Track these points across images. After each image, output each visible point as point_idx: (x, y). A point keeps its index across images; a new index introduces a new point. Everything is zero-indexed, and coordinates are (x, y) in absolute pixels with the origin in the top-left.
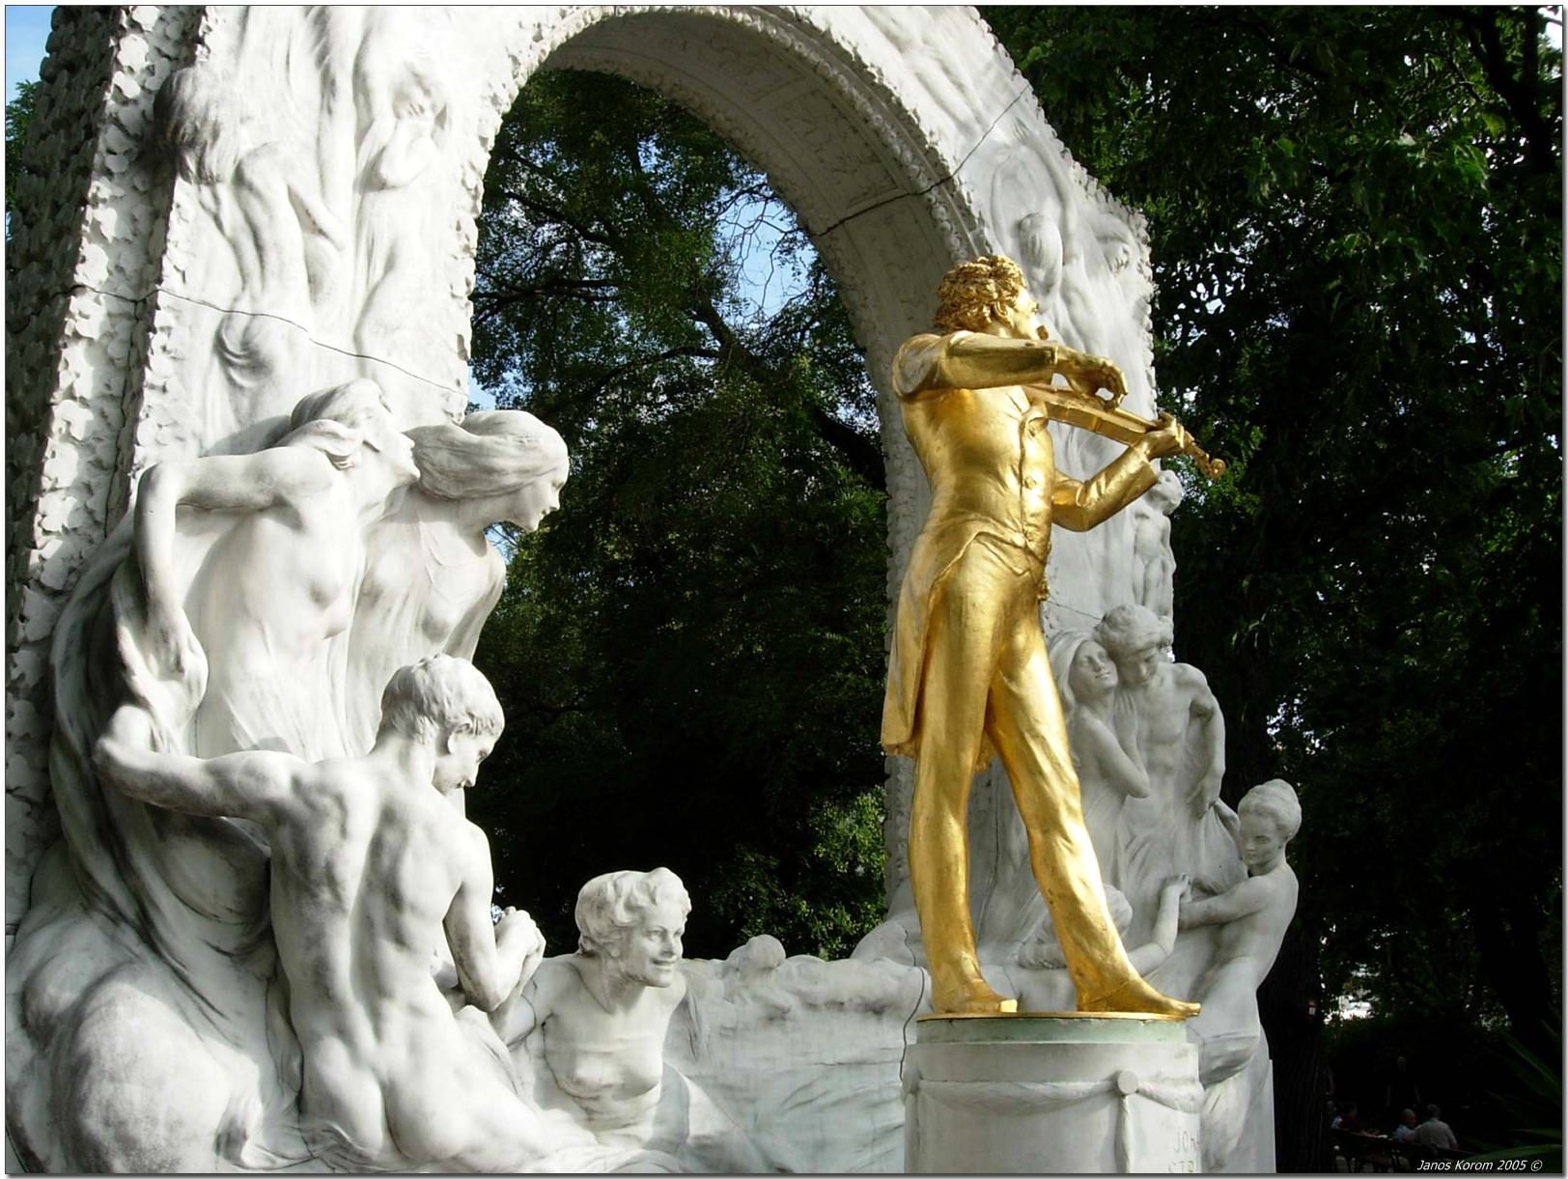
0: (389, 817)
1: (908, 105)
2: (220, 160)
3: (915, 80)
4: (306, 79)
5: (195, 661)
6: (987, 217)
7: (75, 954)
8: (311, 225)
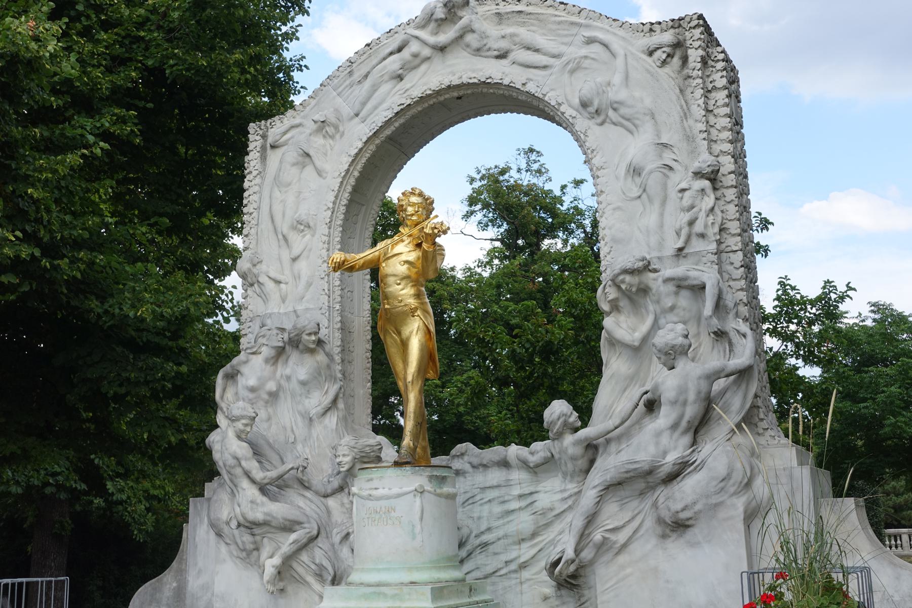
1: (506, 82)
3: (514, 65)
8: (278, 282)
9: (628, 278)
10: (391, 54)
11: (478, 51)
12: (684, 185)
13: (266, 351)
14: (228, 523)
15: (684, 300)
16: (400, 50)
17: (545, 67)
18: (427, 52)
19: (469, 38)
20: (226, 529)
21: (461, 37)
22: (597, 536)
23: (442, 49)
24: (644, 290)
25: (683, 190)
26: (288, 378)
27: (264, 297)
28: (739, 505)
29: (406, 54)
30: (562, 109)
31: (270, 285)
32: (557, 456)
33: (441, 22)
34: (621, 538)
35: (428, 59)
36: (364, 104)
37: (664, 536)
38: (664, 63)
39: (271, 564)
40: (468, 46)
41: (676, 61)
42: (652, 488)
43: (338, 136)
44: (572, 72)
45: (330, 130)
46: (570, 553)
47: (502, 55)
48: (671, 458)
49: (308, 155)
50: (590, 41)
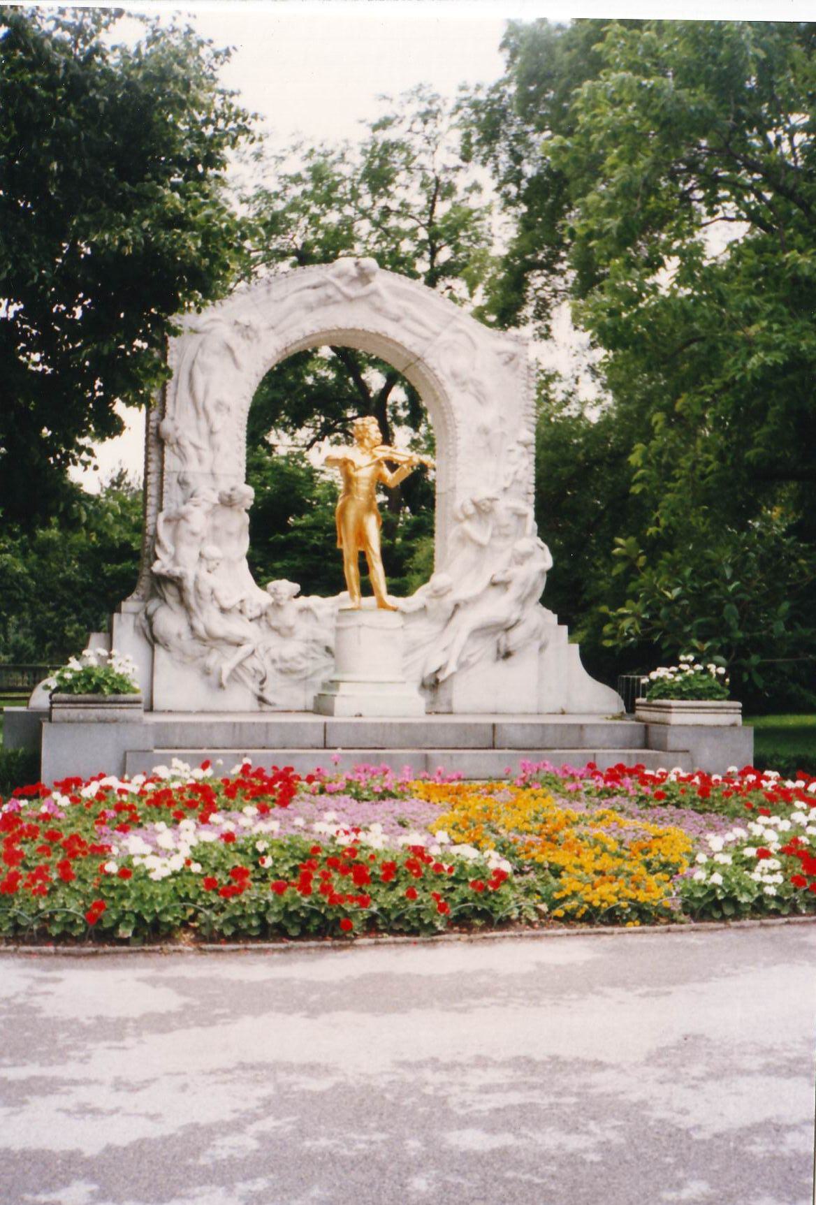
0: (197, 577)
1: (398, 340)
2: (172, 440)
4: (192, 412)
5: (171, 549)
6: (435, 365)
7: (153, 605)
8: (196, 447)
9: (488, 503)
10: (308, 287)
11: (378, 310)
12: (510, 447)
13: (206, 506)
14: (179, 635)
15: (513, 522)
16: (315, 287)
17: (427, 339)
18: (339, 297)
19: (374, 299)
20: (174, 640)
21: (367, 296)
22: (463, 659)
23: (350, 299)
24: (491, 510)
25: (510, 451)
26: (215, 528)
27: (183, 457)
28: (537, 644)
29: (321, 292)
30: (437, 372)
31: (190, 451)
32: (430, 607)
33: (354, 280)
34: (473, 660)
35: (336, 302)
36: (281, 321)
37: (497, 659)
38: (506, 363)
39: (227, 667)
40: (372, 304)
41: (513, 363)
42: (495, 634)
43: (255, 341)
44: (446, 349)
45: (251, 334)
46: (452, 668)
47: (397, 320)
48: (514, 617)
49: (229, 349)
50: (459, 331)
